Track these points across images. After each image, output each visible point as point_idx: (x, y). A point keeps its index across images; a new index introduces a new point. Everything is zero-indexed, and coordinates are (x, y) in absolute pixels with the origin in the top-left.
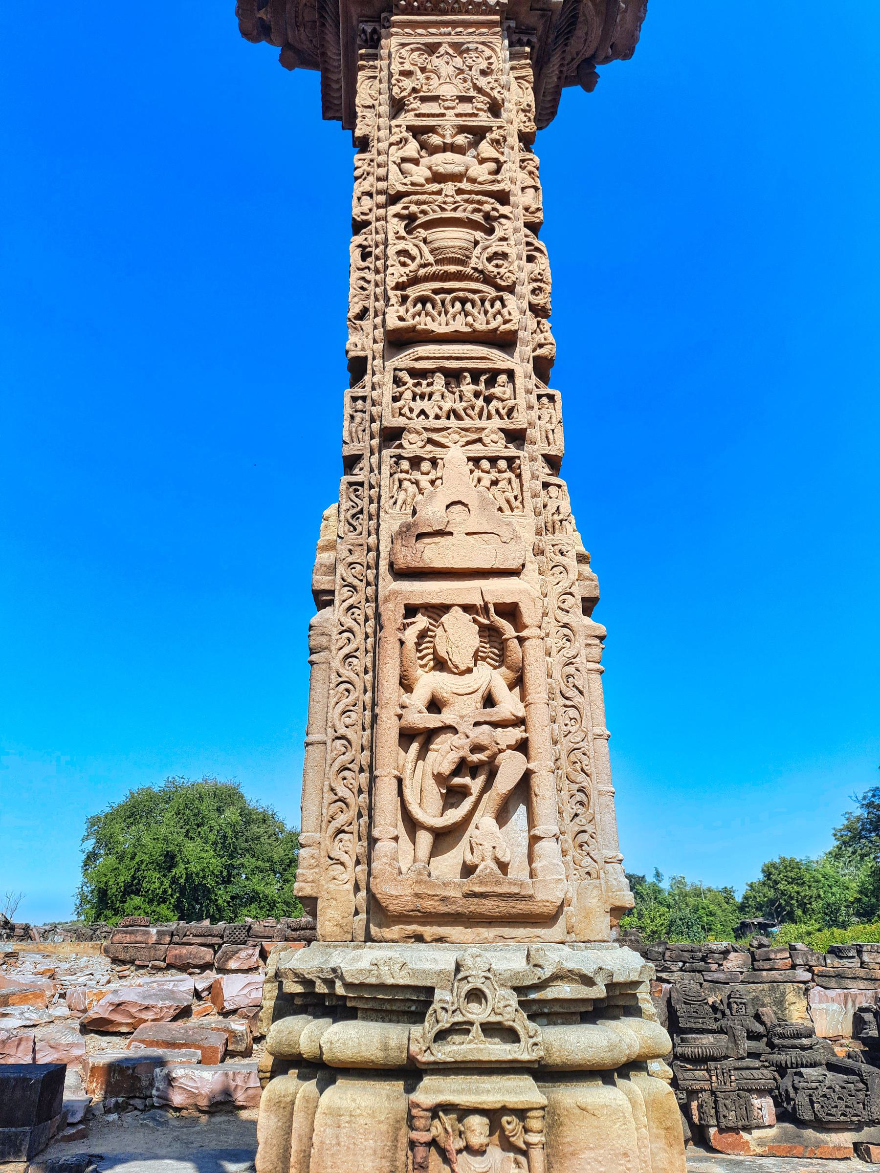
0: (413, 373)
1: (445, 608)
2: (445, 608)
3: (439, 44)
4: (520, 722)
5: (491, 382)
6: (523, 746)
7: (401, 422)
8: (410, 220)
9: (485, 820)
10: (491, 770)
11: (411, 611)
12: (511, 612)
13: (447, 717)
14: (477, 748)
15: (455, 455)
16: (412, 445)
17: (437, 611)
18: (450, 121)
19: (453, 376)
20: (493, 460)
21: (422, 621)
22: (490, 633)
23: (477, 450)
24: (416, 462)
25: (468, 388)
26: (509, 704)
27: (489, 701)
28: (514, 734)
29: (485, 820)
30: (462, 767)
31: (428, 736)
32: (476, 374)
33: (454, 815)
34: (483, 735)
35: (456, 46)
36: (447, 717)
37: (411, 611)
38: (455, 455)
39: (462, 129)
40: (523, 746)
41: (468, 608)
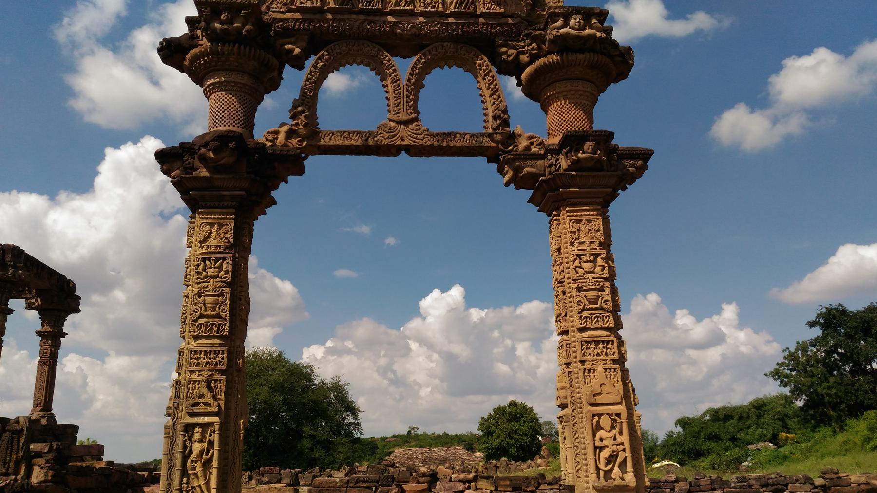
0: (586, 342)
1: (602, 414)
2: (602, 414)
3: (581, 221)
4: (622, 444)
5: (607, 344)
6: (624, 450)
7: (584, 358)
8: (579, 289)
9: (616, 468)
10: (617, 456)
11: (594, 415)
12: (618, 415)
13: (605, 443)
14: (613, 451)
15: (600, 368)
16: (588, 366)
17: (600, 415)
18: (589, 252)
19: (597, 343)
20: (610, 369)
21: (596, 418)
22: (614, 420)
23: (606, 366)
24: (589, 370)
25: (601, 346)
26: (620, 439)
27: (615, 439)
28: (621, 447)
29: (616, 468)
30: (611, 456)
31: (601, 449)
32: (603, 342)
33: (610, 467)
34: (615, 448)
35: (586, 220)
36: (605, 443)
37: (594, 415)
38: (600, 368)
39: (591, 255)
40: (624, 450)
41: (610, 415)
